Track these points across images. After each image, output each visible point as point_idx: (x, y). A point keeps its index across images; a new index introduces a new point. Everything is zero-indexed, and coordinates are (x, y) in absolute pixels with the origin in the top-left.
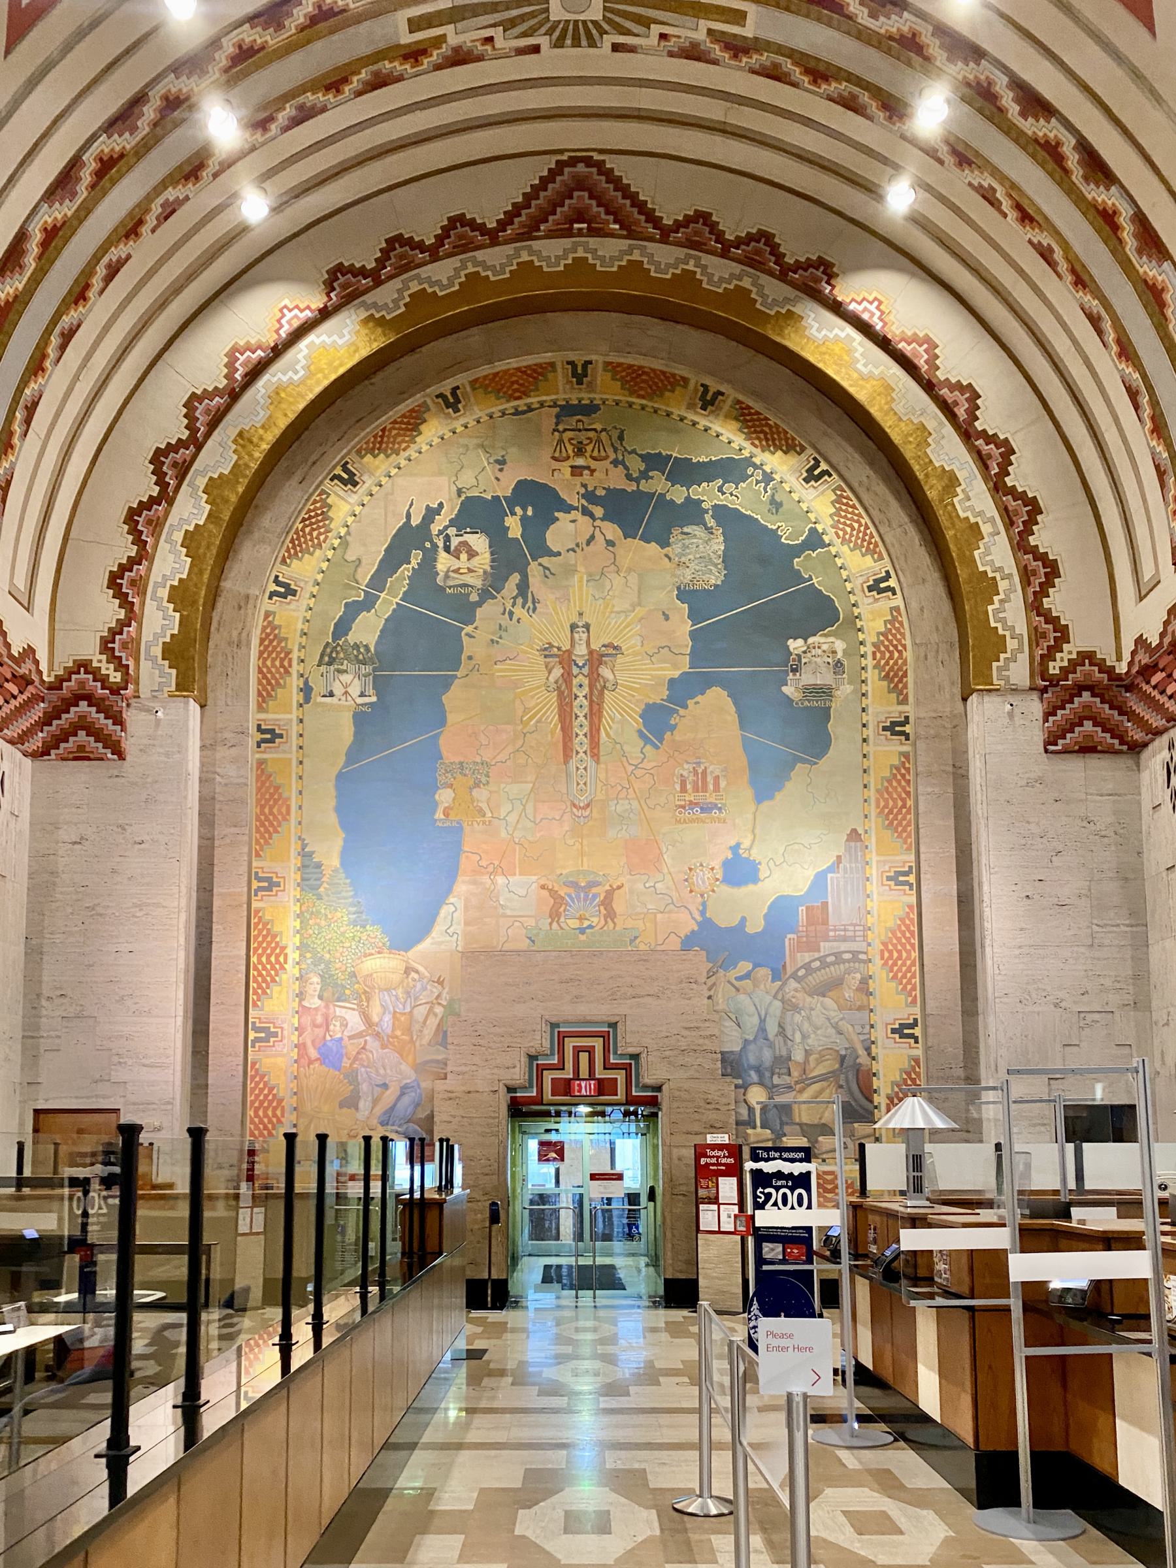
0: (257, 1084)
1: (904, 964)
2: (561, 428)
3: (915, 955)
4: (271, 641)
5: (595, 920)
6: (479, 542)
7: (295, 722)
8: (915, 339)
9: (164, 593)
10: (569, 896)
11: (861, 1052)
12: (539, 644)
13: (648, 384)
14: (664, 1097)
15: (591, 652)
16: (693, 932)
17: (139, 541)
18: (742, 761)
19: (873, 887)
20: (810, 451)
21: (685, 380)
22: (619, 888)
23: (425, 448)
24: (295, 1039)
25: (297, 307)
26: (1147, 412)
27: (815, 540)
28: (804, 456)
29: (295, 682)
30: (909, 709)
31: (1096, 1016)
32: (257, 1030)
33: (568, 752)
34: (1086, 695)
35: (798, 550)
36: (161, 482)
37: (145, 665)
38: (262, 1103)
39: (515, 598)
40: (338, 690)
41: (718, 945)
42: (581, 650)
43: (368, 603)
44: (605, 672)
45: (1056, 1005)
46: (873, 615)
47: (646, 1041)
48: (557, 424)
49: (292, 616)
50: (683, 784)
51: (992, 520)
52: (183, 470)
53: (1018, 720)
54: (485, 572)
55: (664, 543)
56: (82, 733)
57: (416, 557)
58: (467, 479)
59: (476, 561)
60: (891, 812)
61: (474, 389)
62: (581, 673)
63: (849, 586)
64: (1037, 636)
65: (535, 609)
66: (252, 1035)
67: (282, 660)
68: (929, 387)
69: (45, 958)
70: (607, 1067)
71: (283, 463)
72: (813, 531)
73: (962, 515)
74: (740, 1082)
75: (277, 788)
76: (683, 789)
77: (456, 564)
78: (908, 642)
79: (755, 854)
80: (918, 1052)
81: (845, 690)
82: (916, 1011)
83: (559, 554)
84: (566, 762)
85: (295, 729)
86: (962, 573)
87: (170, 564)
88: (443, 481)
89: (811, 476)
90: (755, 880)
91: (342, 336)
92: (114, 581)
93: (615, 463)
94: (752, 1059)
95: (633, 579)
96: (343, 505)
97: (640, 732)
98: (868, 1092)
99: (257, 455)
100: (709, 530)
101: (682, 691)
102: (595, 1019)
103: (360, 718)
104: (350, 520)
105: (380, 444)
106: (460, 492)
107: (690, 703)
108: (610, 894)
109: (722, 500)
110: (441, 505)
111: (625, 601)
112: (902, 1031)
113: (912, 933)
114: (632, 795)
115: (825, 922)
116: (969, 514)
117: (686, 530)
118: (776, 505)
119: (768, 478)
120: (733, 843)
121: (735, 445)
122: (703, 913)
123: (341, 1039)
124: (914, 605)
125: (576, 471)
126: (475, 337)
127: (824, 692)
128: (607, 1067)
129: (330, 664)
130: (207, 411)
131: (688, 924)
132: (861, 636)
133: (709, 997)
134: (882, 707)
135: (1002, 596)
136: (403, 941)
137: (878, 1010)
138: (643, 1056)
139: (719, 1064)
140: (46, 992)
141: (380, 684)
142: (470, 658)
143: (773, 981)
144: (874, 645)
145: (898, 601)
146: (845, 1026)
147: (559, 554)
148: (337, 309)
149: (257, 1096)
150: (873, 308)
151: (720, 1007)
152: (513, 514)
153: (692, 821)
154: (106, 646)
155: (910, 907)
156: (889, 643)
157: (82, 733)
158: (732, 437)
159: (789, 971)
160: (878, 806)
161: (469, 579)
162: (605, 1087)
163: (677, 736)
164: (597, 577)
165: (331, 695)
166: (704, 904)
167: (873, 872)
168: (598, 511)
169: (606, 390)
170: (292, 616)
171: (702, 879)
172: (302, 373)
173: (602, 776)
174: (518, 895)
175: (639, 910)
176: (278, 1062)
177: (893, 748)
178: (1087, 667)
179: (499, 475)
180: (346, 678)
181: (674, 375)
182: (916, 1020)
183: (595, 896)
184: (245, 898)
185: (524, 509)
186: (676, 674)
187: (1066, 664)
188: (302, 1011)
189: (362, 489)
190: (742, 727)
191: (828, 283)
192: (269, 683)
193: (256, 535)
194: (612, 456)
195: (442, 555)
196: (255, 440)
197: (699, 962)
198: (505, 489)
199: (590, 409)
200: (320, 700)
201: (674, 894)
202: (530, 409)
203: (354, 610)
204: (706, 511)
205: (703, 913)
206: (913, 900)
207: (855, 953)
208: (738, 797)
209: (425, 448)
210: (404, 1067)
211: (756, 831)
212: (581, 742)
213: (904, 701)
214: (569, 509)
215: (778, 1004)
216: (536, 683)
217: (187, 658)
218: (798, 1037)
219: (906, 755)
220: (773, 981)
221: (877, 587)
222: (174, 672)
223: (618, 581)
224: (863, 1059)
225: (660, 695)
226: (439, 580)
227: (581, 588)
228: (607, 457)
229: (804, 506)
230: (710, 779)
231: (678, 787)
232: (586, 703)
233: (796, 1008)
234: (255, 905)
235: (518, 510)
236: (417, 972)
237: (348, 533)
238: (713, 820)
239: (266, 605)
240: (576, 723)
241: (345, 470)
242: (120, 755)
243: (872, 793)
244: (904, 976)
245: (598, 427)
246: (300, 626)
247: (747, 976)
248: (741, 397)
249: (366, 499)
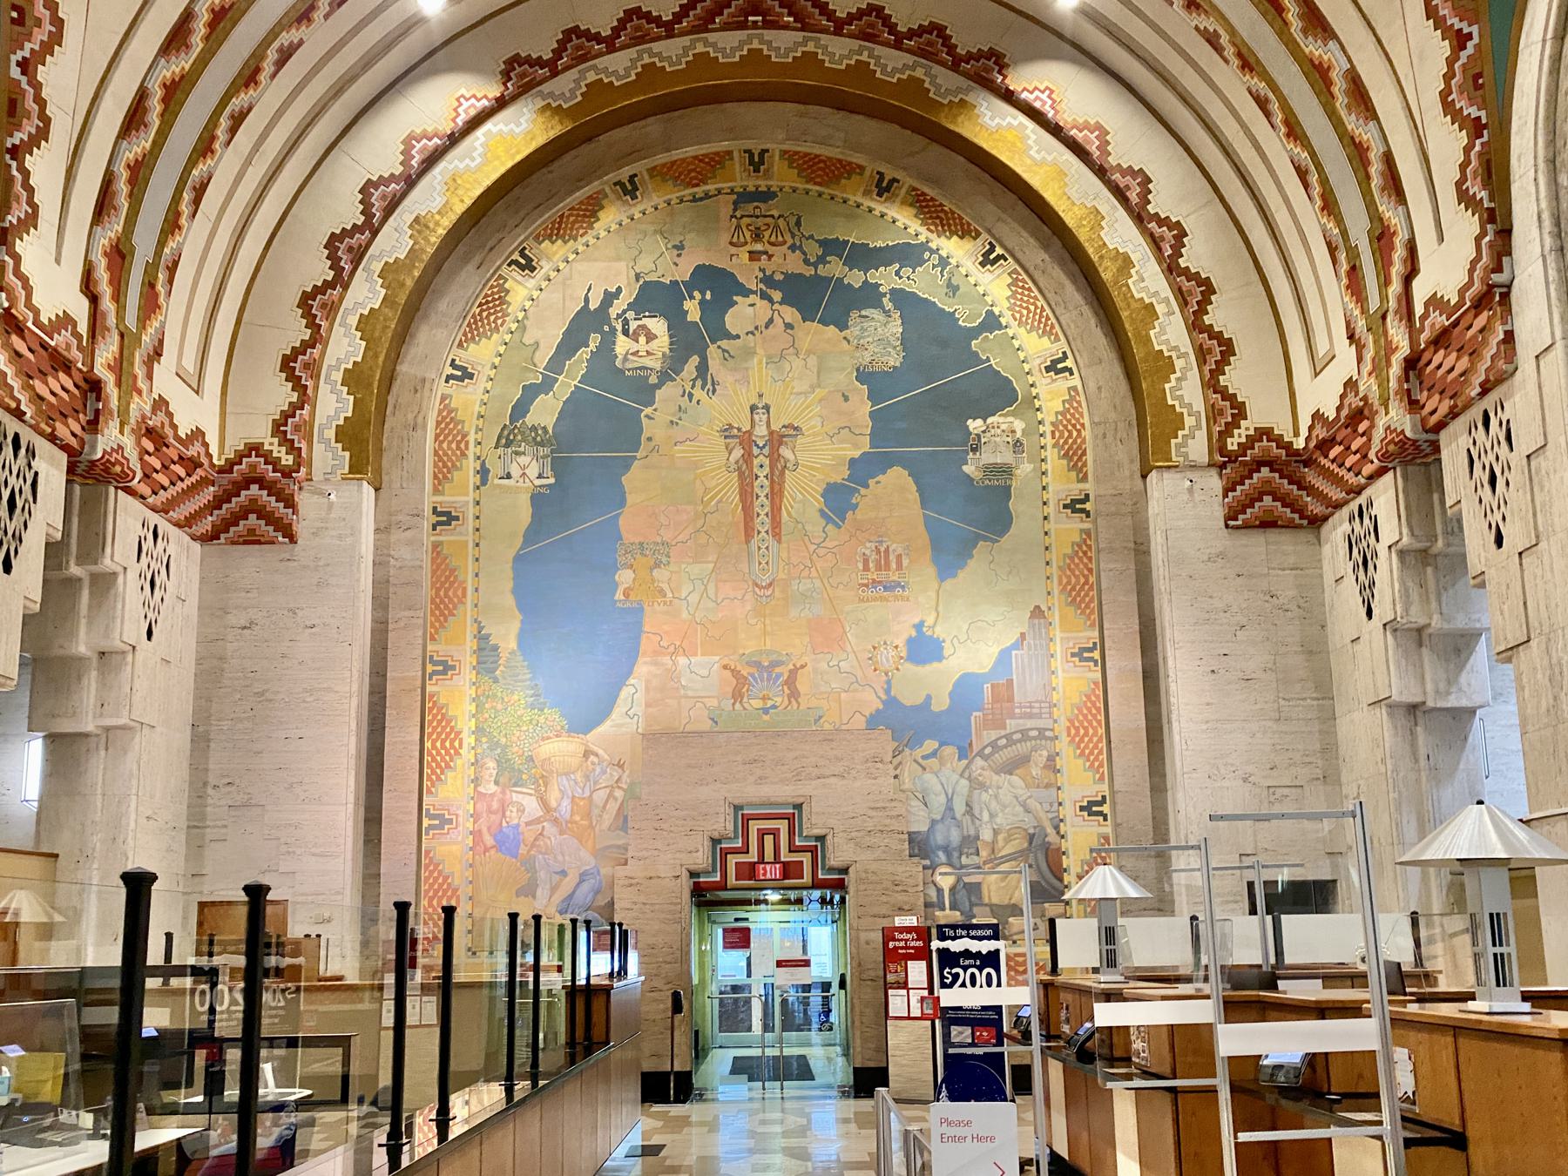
0: (431, 872)
1: (1091, 740)
2: (738, 214)
3: (1102, 731)
4: (447, 424)
5: (779, 699)
6: (658, 326)
7: (471, 505)
8: (1086, 126)
9: (338, 376)
10: (752, 675)
11: (1050, 830)
12: (718, 425)
13: (827, 171)
14: (851, 880)
15: (771, 433)
16: (878, 710)
17: (312, 324)
18: (923, 538)
19: (1058, 663)
20: (984, 235)
21: (862, 168)
22: (803, 667)
23: (603, 234)
24: (470, 825)
25: (474, 96)
26: (1316, 190)
27: (991, 322)
28: (979, 241)
29: (471, 465)
30: (1089, 487)
31: (1286, 791)
32: (432, 817)
33: (749, 532)
34: (1265, 471)
35: (975, 333)
36: (335, 266)
37: (318, 448)
38: (436, 892)
39: (694, 380)
40: (515, 470)
41: (904, 726)
42: (761, 431)
43: (547, 385)
44: (785, 452)
45: (1245, 780)
46: (1051, 395)
47: (832, 822)
48: (735, 210)
49: (468, 399)
50: (866, 562)
51: (1167, 301)
52: (358, 255)
53: (1198, 496)
54: (664, 355)
55: (843, 326)
56: (253, 517)
57: (594, 341)
58: (645, 264)
59: (654, 344)
60: (1073, 589)
61: (651, 177)
62: (761, 453)
63: (1026, 367)
64: (1213, 413)
65: (714, 391)
66: (426, 822)
67: (459, 443)
68: (1101, 172)
69: (212, 745)
70: (793, 849)
71: (461, 248)
72: (990, 313)
73: (1137, 296)
74: (927, 862)
75: (453, 571)
76: (866, 568)
77: (634, 347)
78: (1086, 420)
79: (939, 632)
80: (1108, 829)
81: (1025, 469)
82: (1104, 788)
83: (738, 337)
84: (747, 542)
85: (471, 511)
86: (1138, 352)
87: (344, 347)
88: (622, 266)
89: (987, 260)
90: (939, 657)
91: (518, 125)
92: (287, 364)
93: (793, 248)
94: (939, 838)
95: (813, 361)
96: (520, 289)
97: (821, 511)
98: (1058, 872)
99: (433, 239)
100: (887, 313)
101: (863, 470)
102: (780, 800)
103: (537, 499)
104: (528, 304)
105: (558, 231)
106: (638, 277)
107: (871, 482)
108: (793, 673)
109: (898, 284)
110: (619, 290)
112: (1090, 808)
113: (1098, 710)
114: (814, 574)
115: (1011, 699)
116: (1143, 295)
117: (863, 313)
118: (953, 289)
119: (944, 262)
120: (916, 621)
121: (911, 231)
122: (888, 692)
123: (518, 825)
124: (1092, 385)
125: (754, 256)
126: (653, 127)
127: (1005, 471)
128: (793, 849)
129: (507, 445)
130: (383, 197)
131: (872, 701)
132: (1040, 416)
133: (896, 777)
134: (1061, 485)
135: (1178, 374)
136: (582, 724)
137: (1065, 788)
138: (829, 838)
139: (906, 845)
140: (212, 780)
141: (559, 467)
142: (649, 439)
143: (960, 759)
144: (1053, 424)
145: (1075, 381)
146: (1032, 804)
147: (738, 337)
148: (514, 98)
149: (431, 885)
150: (1044, 96)
151: (906, 787)
152: (692, 297)
153: (875, 599)
154: (278, 428)
155: (1096, 684)
156: (1068, 421)
157: (253, 517)
158: (908, 223)
159: (976, 749)
160: (1060, 583)
161: (648, 362)
162: (790, 870)
163: (859, 514)
164: (777, 359)
165: (509, 476)
166: (889, 682)
167: (1058, 648)
168: (777, 296)
169: (782, 177)
170: (468, 399)
171: (887, 657)
172: (479, 160)
173: (784, 555)
174: (702, 674)
175: (823, 689)
176: (452, 850)
177: (1072, 527)
178: (1265, 443)
179: (676, 260)
180: (523, 460)
181: (850, 163)
182: (1104, 797)
183: (781, 675)
184: (419, 683)
185: (703, 294)
186: (857, 454)
187: (1243, 440)
188: (478, 796)
189: (540, 274)
190: (924, 505)
191: (1000, 72)
192: (445, 466)
193: (433, 318)
194: (790, 242)
195: (621, 338)
196: (431, 225)
197: (884, 743)
198: (684, 272)
199: (766, 196)
200: (497, 481)
201: (859, 674)
202: (707, 196)
203: (531, 393)
204: (884, 295)
205: (888, 692)
206: (1099, 675)
207: (1041, 731)
208: (921, 575)
209: (603, 234)
210: (585, 854)
211: (940, 608)
212: (762, 522)
213: (1084, 479)
214: (746, 293)
215: (964, 782)
216: (716, 466)
217: (363, 443)
218: (986, 816)
219: (1088, 533)
220: (960, 759)
221: (1053, 367)
222: (347, 454)
223: (797, 363)
224: (1052, 837)
225: (841, 475)
226: (618, 363)
227: (760, 370)
228: (785, 242)
229: (981, 290)
230: (892, 557)
231: (861, 566)
232: (767, 483)
233: (983, 786)
234: (428, 689)
235: (697, 294)
236: (597, 755)
237: (526, 317)
238: (896, 598)
239: (442, 388)
240: (757, 503)
241: (522, 254)
242: (291, 538)
243: (1054, 570)
244: (1091, 753)
245: (776, 213)
246: (477, 408)
247: (934, 754)
248: (916, 184)
249: (544, 284)
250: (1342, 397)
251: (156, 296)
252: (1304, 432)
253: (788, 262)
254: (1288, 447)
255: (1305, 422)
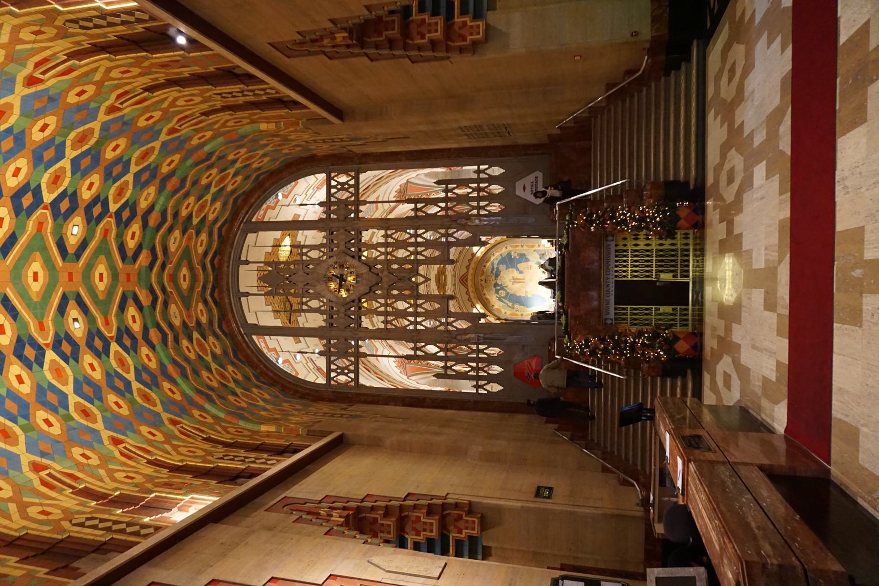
46: (509, 248)
62: (515, 280)
101: (517, 269)
105: (489, 302)
111: (508, 277)
134: (520, 248)
156: (512, 247)
169: (483, 277)
253: (493, 277)
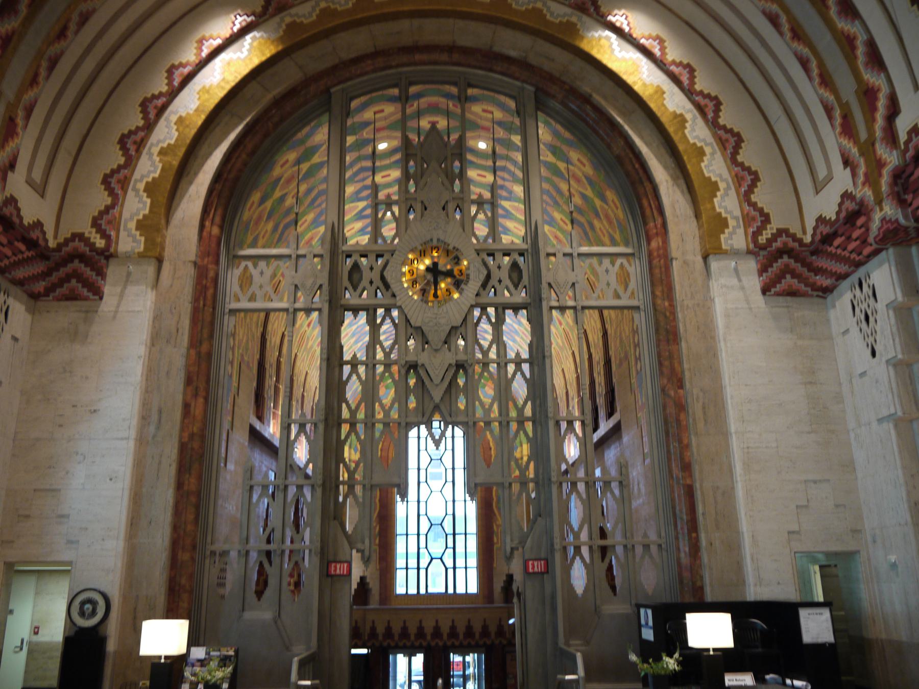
56: (74, 281)
157: (74, 281)
187: (770, 236)
222: (143, 239)
242: (101, 298)
250: (840, 205)
251: (15, 125)
252: (810, 231)
254: (800, 241)
255: (810, 224)
